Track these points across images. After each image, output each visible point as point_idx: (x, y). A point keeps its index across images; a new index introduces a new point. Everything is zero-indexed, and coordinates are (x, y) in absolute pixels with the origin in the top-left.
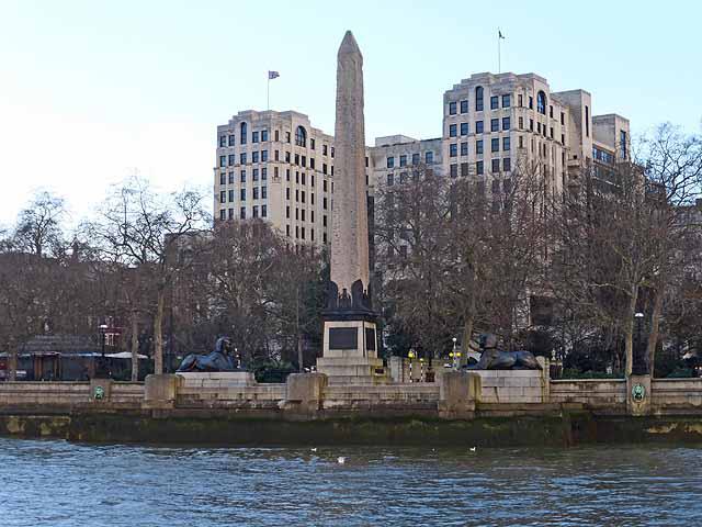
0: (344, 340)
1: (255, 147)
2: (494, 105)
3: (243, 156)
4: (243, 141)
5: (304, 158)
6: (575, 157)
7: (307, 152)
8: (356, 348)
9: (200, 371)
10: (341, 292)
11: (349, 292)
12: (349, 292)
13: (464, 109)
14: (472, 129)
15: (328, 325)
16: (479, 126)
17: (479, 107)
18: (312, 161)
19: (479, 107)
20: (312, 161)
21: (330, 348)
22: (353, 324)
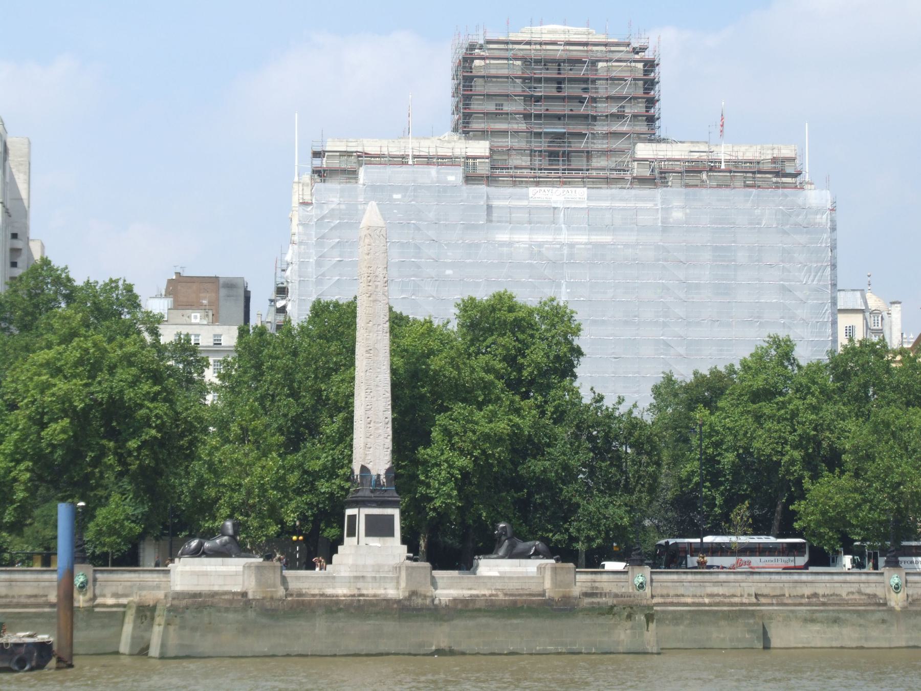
0: (378, 527)
6: (14, 236)
8: (391, 534)
11: (383, 478)
12: (383, 478)
15: (365, 511)
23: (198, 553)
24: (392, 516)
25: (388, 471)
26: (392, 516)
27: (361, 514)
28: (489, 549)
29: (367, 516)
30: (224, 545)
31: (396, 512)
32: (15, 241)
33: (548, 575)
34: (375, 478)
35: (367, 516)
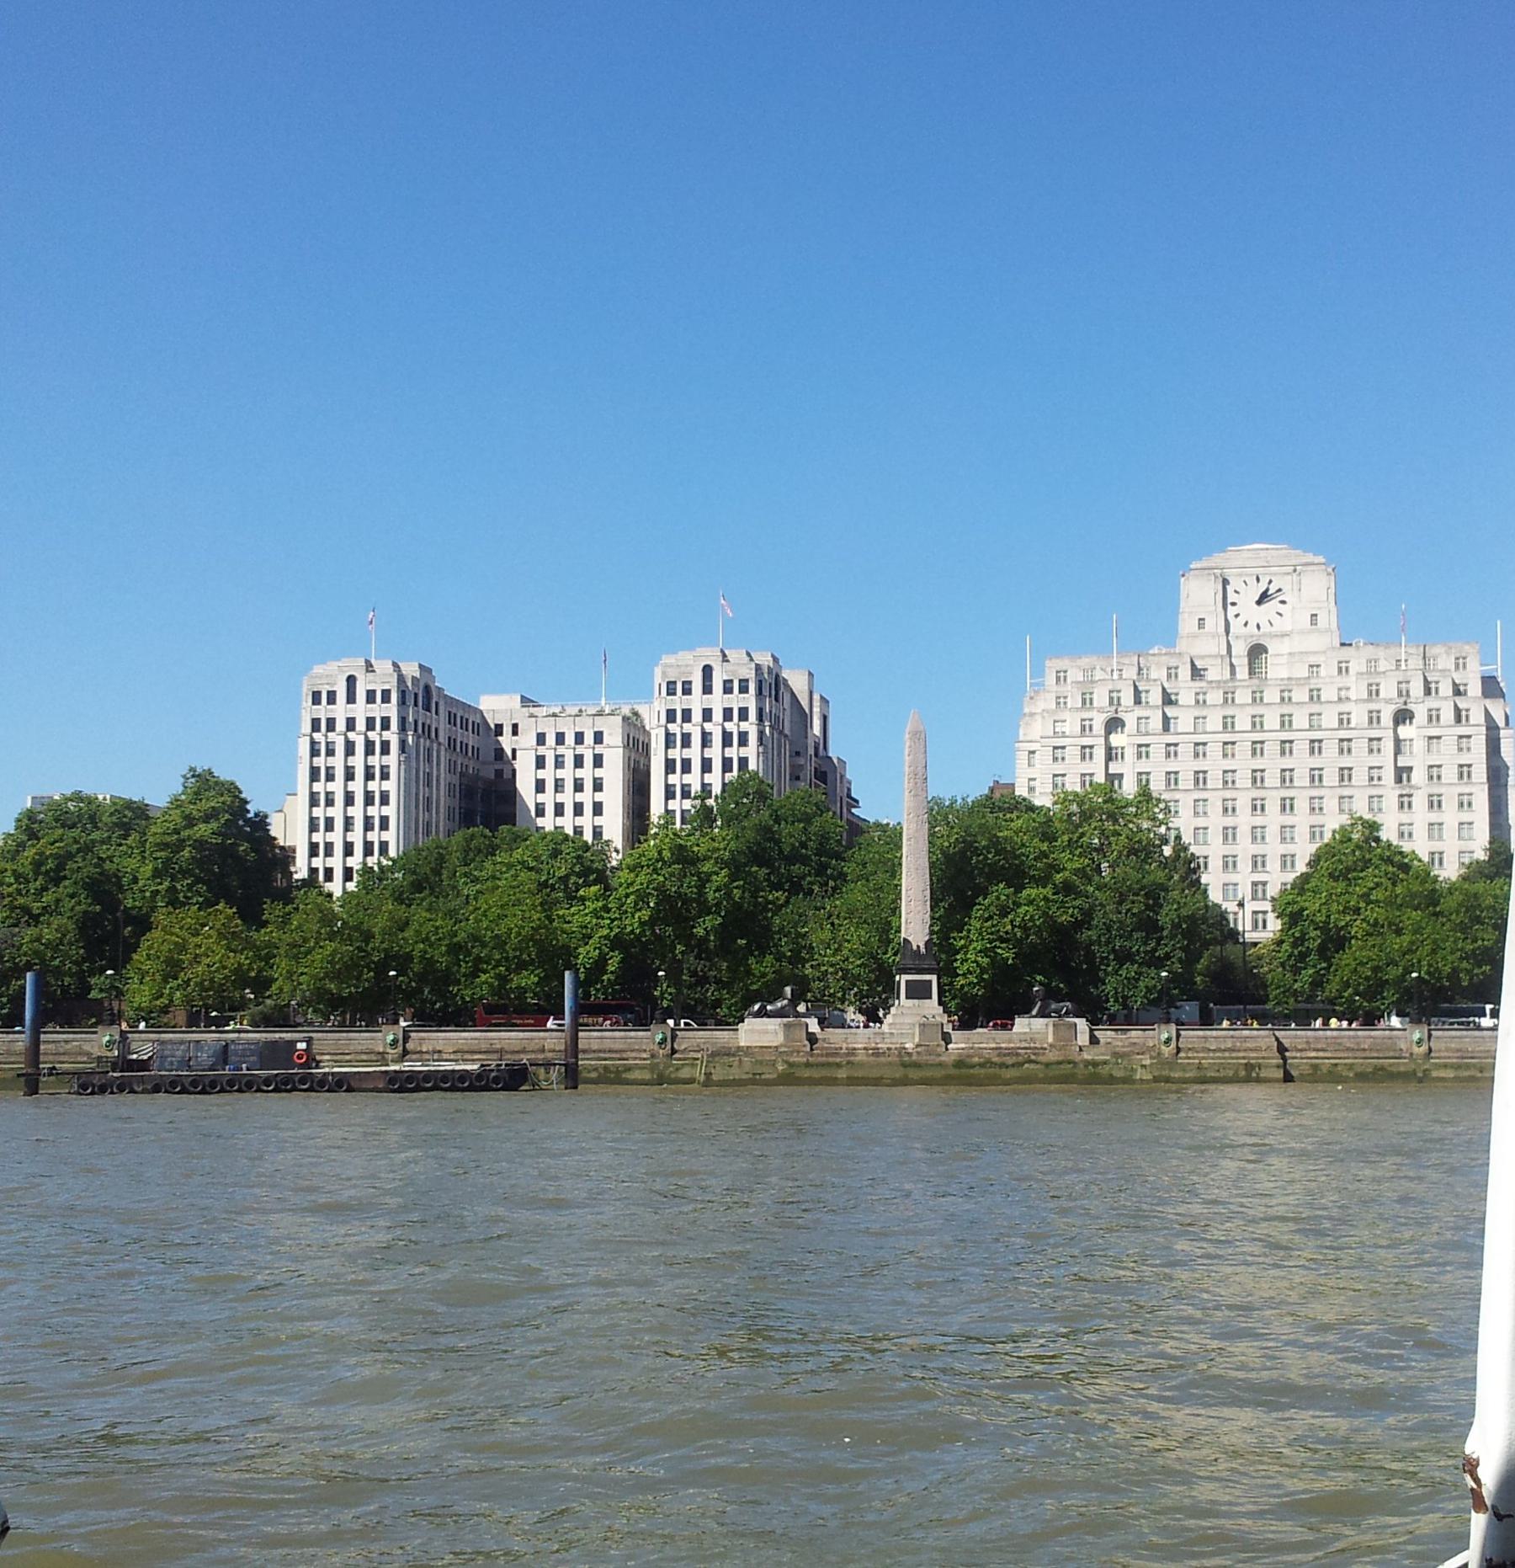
0: (918, 992)
1: (372, 710)
2: (728, 689)
3: (351, 724)
4: (351, 699)
5: (429, 727)
6: (798, 754)
7: (432, 719)
8: (930, 998)
9: (769, 1017)
10: (915, 948)
11: (923, 950)
13: (687, 691)
14: (697, 716)
15: (905, 977)
16: (707, 715)
17: (707, 689)
18: (436, 730)
19: (707, 689)
20: (436, 730)
21: (907, 998)
22: (927, 977)
23: (762, 1014)
24: (930, 981)
25: (927, 944)
26: (930, 981)
27: (903, 979)
28: (1025, 1011)
29: (907, 981)
30: (783, 1008)
31: (934, 978)
32: (797, 759)
33: (1051, 1028)
34: (915, 948)
35: (907, 981)
